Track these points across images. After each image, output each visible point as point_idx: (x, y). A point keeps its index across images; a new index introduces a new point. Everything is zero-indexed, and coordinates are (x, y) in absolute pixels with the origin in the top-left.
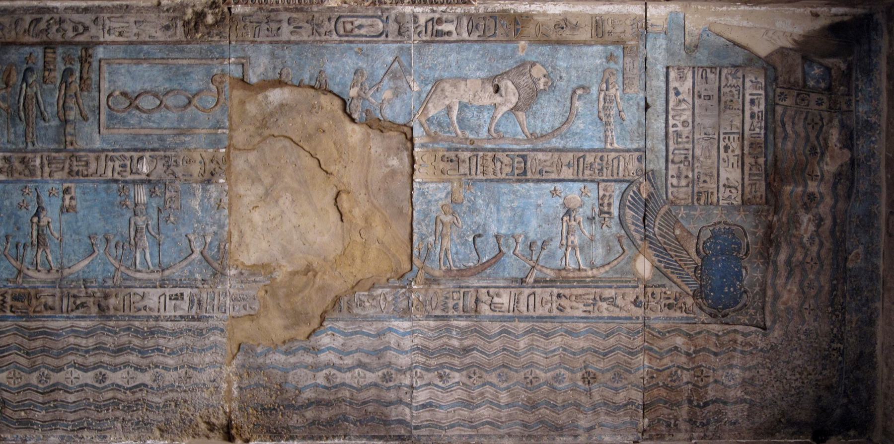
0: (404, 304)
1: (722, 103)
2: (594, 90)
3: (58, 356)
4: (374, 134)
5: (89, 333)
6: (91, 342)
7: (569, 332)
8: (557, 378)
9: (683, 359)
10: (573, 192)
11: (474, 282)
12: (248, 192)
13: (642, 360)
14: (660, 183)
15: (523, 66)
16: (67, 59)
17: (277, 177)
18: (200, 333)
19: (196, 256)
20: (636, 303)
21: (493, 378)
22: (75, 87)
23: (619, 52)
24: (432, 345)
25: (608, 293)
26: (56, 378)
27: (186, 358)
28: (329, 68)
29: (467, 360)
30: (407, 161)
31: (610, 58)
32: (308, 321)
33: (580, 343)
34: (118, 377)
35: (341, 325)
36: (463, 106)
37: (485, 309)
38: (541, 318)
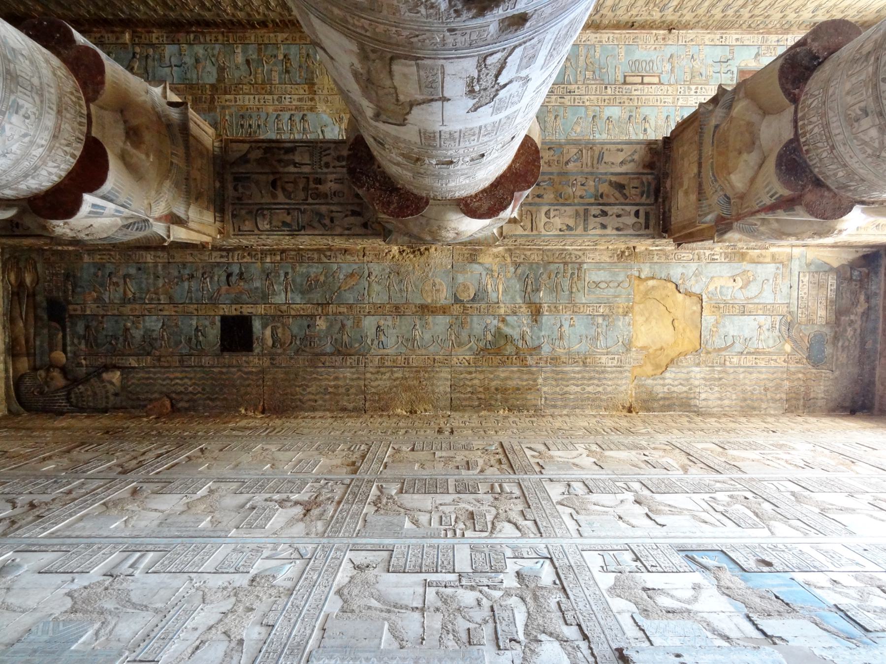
0: (697, 361)
1: (820, 285)
2: (771, 281)
3: (567, 381)
4: (687, 297)
5: (579, 372)
6: (580, 376)
7: (759, 372)
8: (754, 389)
9: (801, 383)
10: (761, 319)
11: (724, 353)
12: (640, 319)
13: (786, 383)
14: (795, 316)
15: (745, 272)
16: (573, 269)
17: (651, 313)
18: (621, 372)
19: (620, 343)
20: (785, 361)
21: (730, 389)
22: (576, 279)
23: (780, 266)
24: (708, 377)
25: (774, 357)
26: (566, 389)
27: (616, 381)
28: (672, 273)
29: (721, 382)
30: (699, 307)
31: (778, 268)
32: (661, 367)
33: (763, 376)
34: (590, 389)
35: (673, 369)
36: (721, 287)
37: (728, 363)
38: (749, 367)
